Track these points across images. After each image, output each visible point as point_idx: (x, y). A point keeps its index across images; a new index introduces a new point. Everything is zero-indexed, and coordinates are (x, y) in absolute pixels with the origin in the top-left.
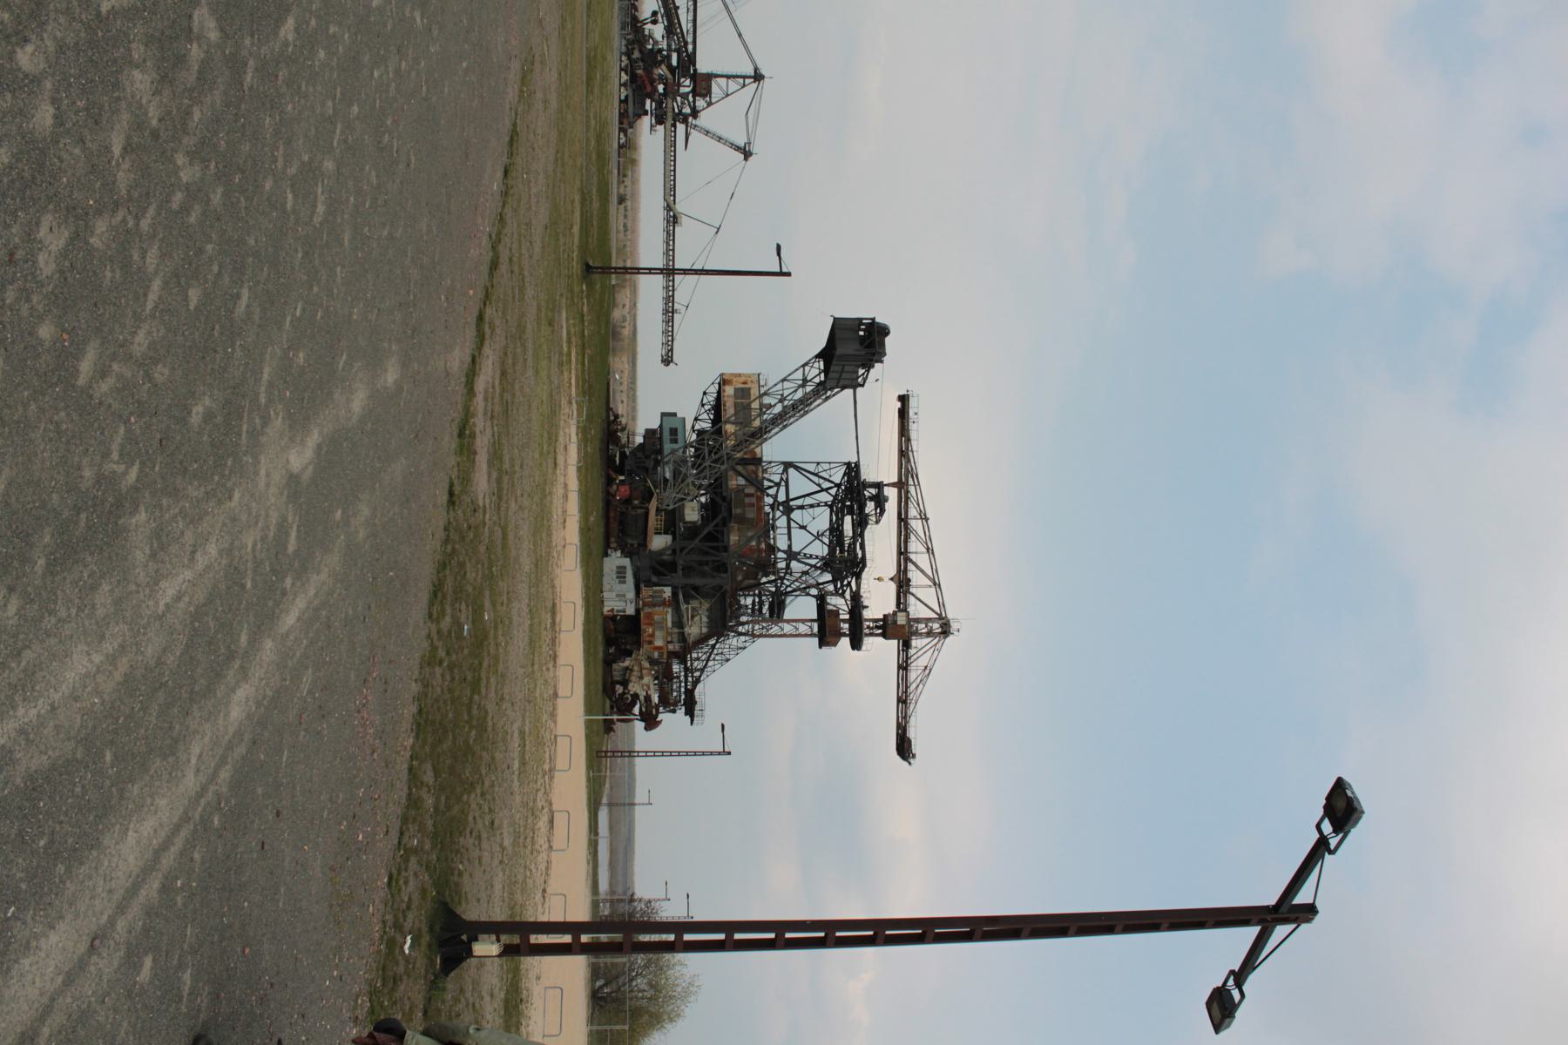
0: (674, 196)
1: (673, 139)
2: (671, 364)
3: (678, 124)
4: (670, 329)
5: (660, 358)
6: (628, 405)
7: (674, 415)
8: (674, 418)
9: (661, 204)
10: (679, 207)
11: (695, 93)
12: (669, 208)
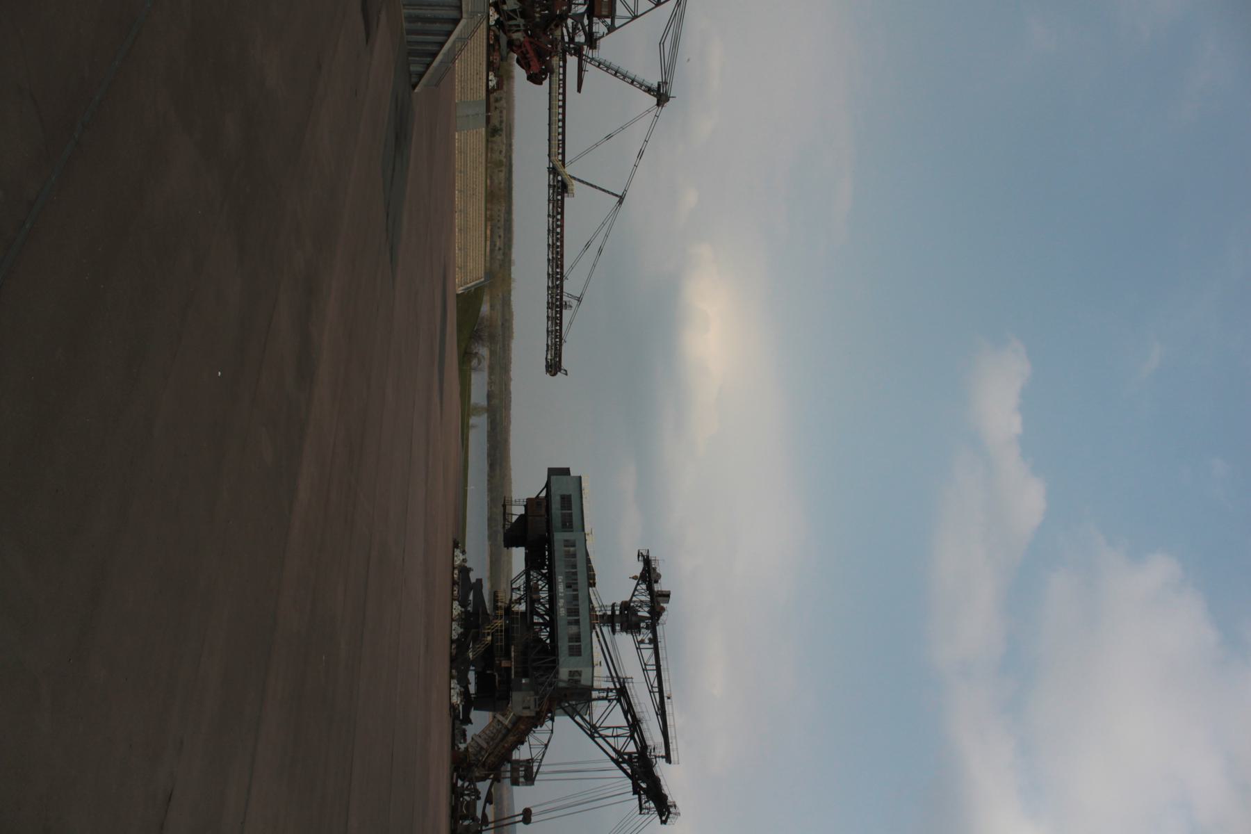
0: (563, 154)
1: (561, 77)
2: (559, 373)
3: (568, 57)
4: (558, 328)
5: (545, 364)
6: (504, 238)
7: (566, 472)
8: (565, 478)
9: (545, 163)
10: (569, 170)
11: (591, 13)
12: (553, 171)
